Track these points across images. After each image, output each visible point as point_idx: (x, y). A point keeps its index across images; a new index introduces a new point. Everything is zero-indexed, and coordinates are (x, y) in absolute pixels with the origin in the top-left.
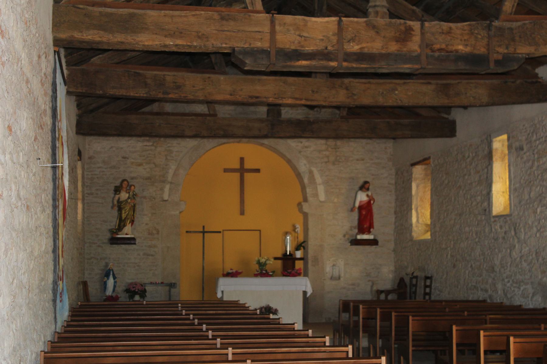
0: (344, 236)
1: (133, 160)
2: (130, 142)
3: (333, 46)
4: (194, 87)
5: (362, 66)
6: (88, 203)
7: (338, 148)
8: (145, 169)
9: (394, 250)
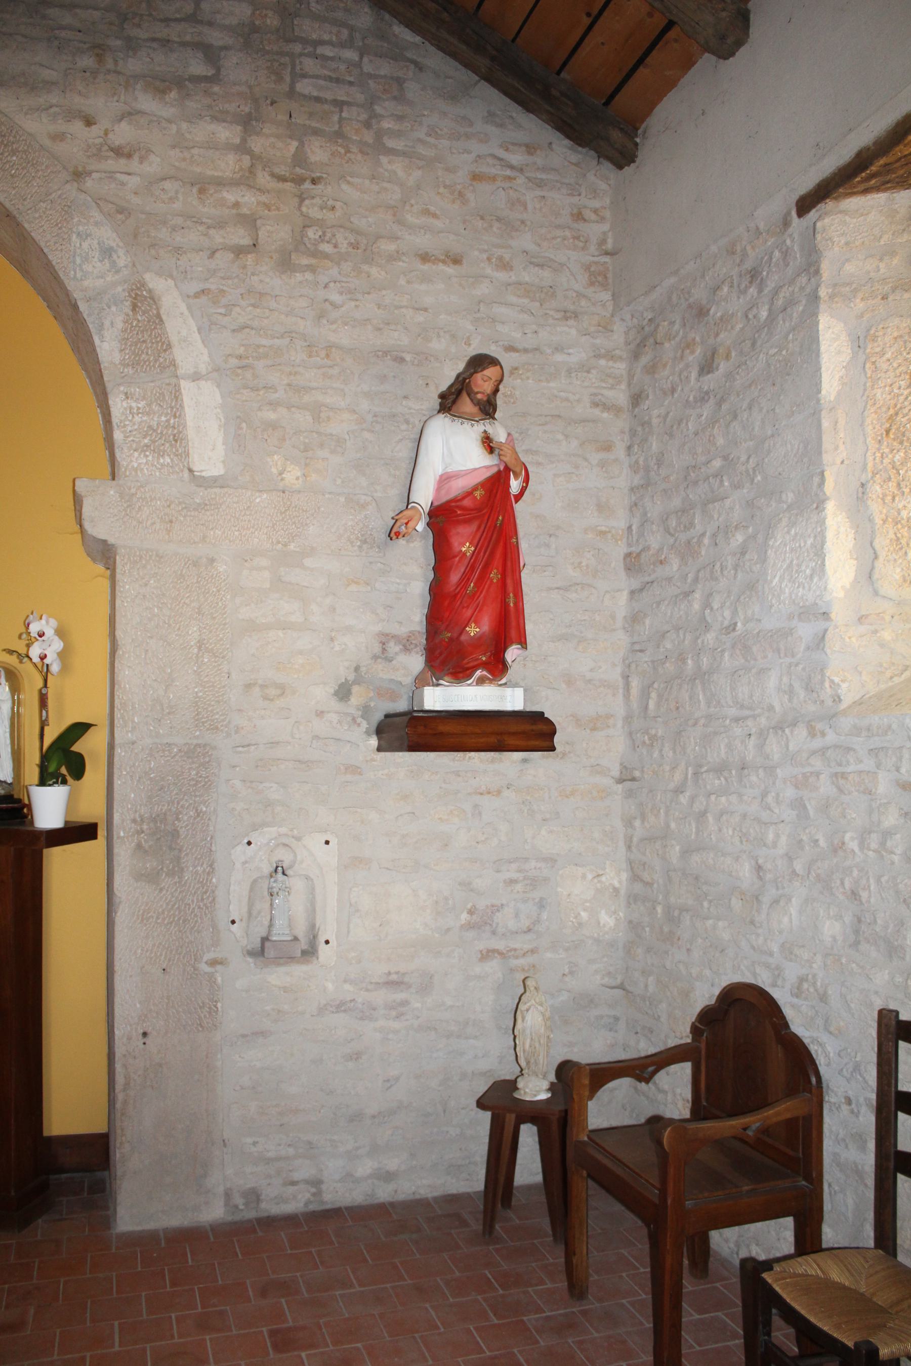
0: (343, 692)
7: (314, 181)
9: (626, 777)
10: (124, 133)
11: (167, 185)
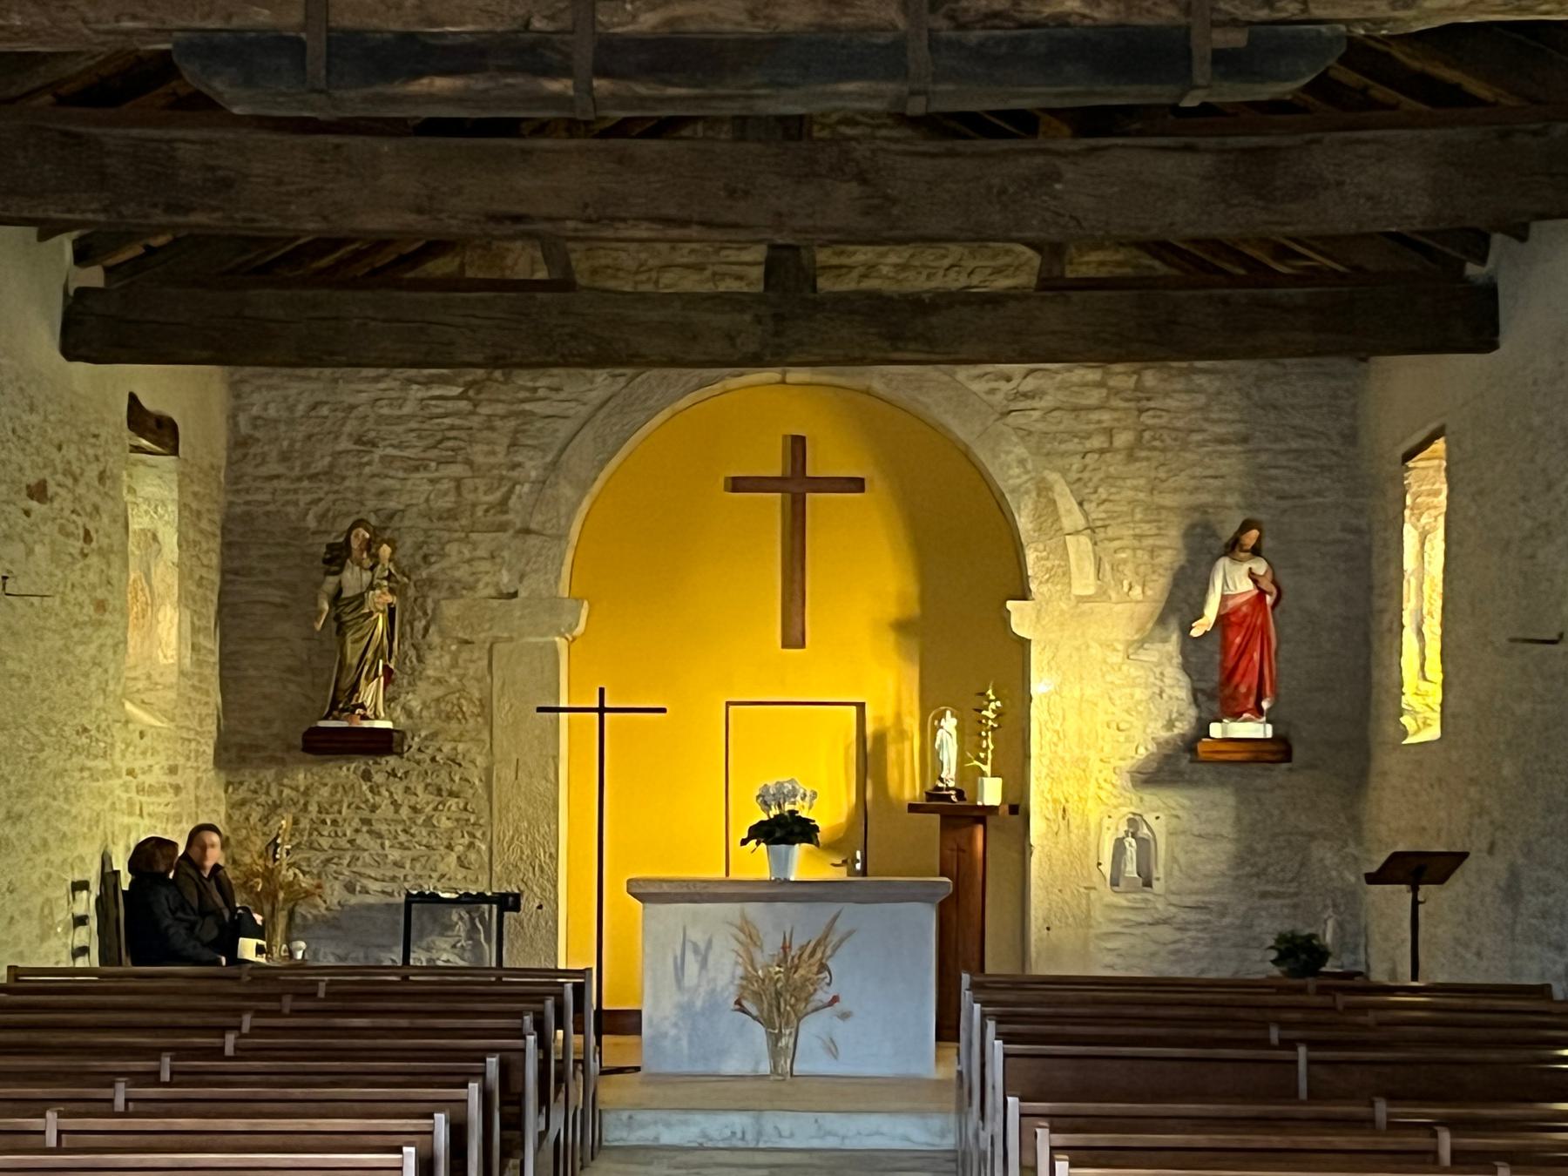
1: (390, 451)
3: (552, 18)
4: (279, 182)
5: (672, 91)
10: (1030, 384)
11: (1055, 414)
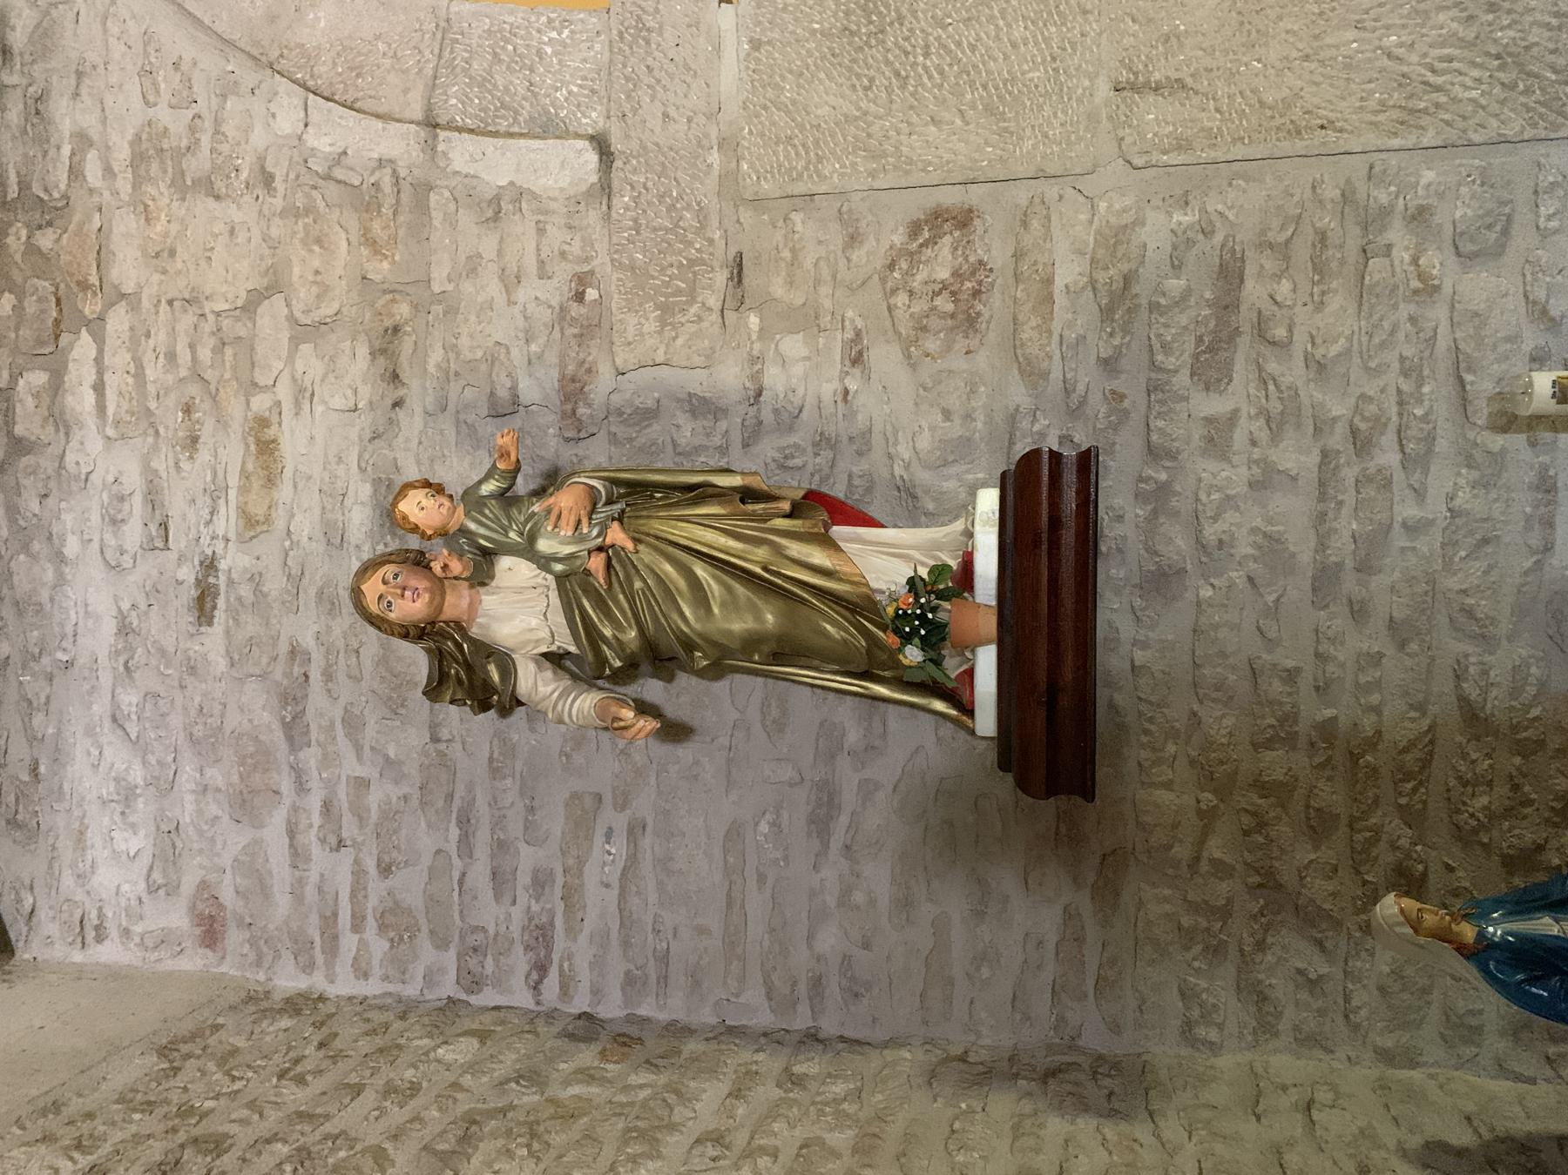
1: (227, 521)
2: (72, 547)
6: (630, 982)
8: (303, 394)
